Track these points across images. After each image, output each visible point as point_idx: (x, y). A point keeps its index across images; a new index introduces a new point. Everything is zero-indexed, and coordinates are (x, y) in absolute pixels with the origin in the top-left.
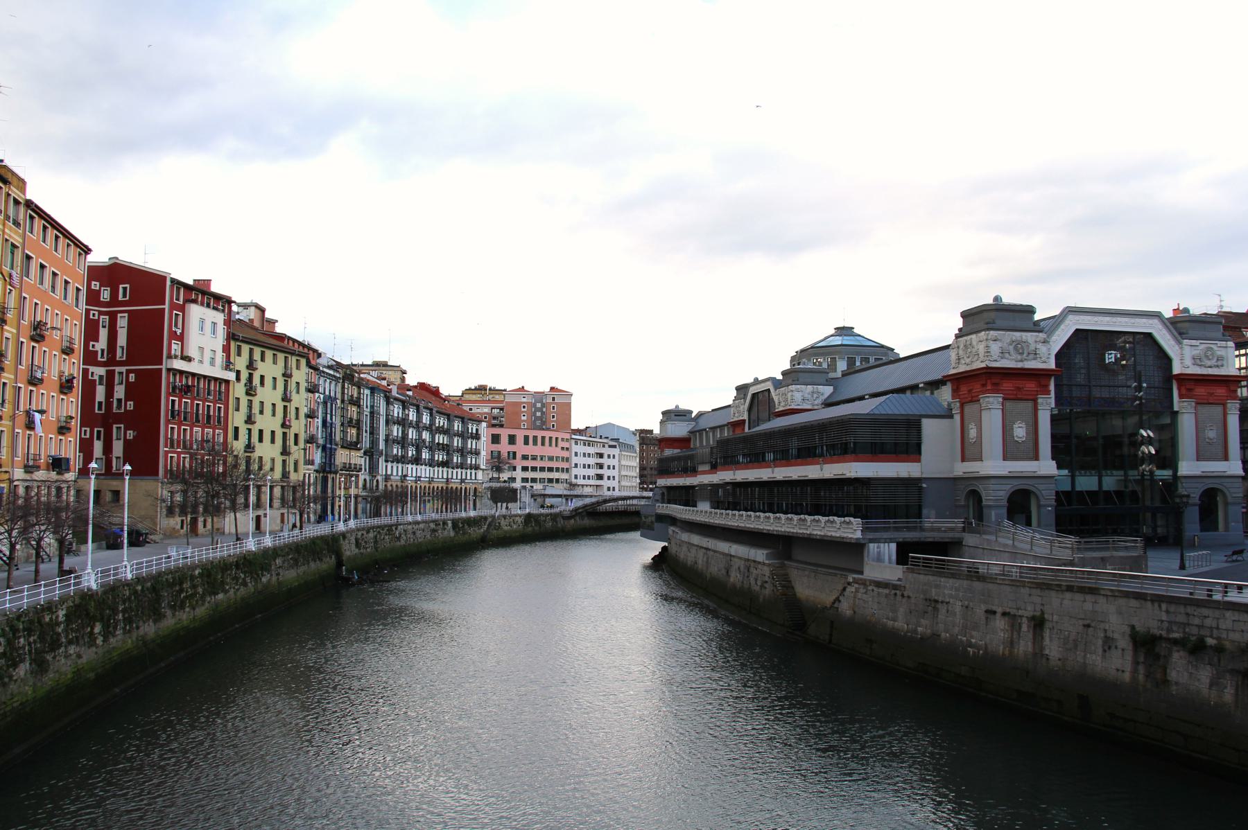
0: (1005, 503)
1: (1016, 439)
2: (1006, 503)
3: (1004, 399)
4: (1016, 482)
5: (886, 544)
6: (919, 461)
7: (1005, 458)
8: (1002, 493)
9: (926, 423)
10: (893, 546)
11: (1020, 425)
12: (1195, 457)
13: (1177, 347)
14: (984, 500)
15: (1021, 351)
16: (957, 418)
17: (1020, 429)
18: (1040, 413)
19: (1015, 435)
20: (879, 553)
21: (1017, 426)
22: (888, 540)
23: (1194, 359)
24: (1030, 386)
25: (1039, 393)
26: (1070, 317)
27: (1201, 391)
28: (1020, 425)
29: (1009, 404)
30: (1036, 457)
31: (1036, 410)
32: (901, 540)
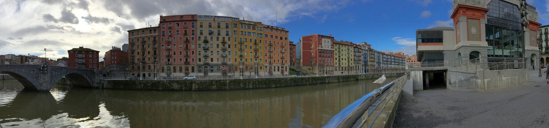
1: (472, 33)
4: (473, 48)
5: (418, 71)
6: (443, 45)
9: (444, 31)
10: (421, 72)
11: (474, 28)
16: (455, 30)
17: (474, 30)
18: (481, 24)
19: (472, 32)
20: (415, 75)
22: (419, 70)
24: (478, 14)
25: (481, 17)
28: (474, 28)
29: (469, 20)
30: (480, 40)
31: (480, 23)
32: (424, 70)
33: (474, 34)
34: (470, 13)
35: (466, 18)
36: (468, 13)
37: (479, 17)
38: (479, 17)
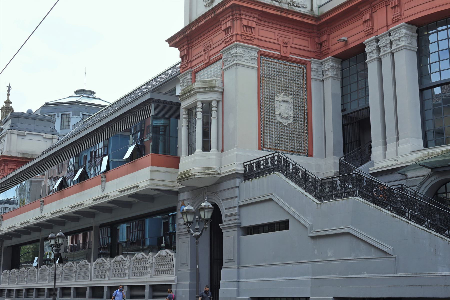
1: (278, 118)
3: (262, 54)
7: (260, 149)
11: (285, 98)
14: (224, 219)
19: (277, 112)
28: (285, 98)
33: (285, 122)
36: (262, 33)
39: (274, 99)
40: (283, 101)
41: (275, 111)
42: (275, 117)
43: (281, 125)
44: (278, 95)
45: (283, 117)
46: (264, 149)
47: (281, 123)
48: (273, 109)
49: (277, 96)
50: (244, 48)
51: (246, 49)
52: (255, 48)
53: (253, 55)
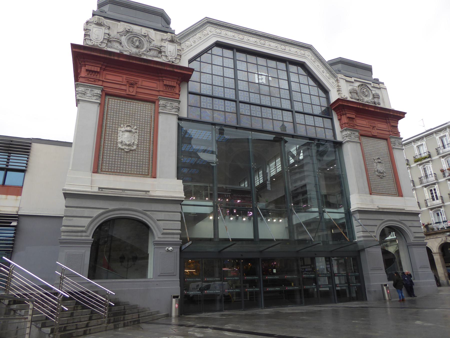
0: (89, 237)
1: (120, 146)
2: (91, 238)
8: (85, 222)
11: (129, 129)
12: (367, 190)
13: (332, 80)
15: (137, 44)
17: (127, 134)
21: (123, 129)
23: (350, 93)
25: (161, 93)
26: (209, 29)
27: (362, 122)
28: (129, 129)
29: (113, 102)
34: (120, 79)
35: (99, 92)
37: (156, 93)
38: (156, 93)
39: (118, 130)
40: (127, 131)
41: (117, 139)
42: (117, 144)
43: (123, 151)
44: (122, 126)
45: (126, 145)
46: (101, 172)
47: (123, 149)
48: (116, 138)
49: (121, 127)
50: (85, 87)
51: (87, 87)
52: (99, 87)
53: (95, 92)
